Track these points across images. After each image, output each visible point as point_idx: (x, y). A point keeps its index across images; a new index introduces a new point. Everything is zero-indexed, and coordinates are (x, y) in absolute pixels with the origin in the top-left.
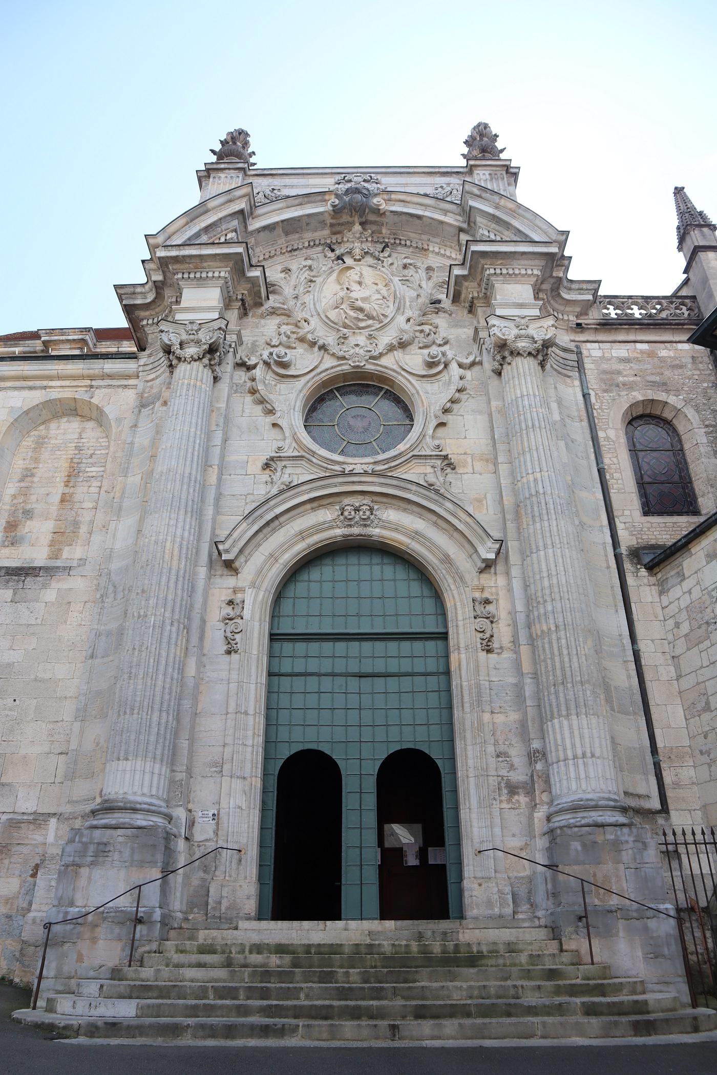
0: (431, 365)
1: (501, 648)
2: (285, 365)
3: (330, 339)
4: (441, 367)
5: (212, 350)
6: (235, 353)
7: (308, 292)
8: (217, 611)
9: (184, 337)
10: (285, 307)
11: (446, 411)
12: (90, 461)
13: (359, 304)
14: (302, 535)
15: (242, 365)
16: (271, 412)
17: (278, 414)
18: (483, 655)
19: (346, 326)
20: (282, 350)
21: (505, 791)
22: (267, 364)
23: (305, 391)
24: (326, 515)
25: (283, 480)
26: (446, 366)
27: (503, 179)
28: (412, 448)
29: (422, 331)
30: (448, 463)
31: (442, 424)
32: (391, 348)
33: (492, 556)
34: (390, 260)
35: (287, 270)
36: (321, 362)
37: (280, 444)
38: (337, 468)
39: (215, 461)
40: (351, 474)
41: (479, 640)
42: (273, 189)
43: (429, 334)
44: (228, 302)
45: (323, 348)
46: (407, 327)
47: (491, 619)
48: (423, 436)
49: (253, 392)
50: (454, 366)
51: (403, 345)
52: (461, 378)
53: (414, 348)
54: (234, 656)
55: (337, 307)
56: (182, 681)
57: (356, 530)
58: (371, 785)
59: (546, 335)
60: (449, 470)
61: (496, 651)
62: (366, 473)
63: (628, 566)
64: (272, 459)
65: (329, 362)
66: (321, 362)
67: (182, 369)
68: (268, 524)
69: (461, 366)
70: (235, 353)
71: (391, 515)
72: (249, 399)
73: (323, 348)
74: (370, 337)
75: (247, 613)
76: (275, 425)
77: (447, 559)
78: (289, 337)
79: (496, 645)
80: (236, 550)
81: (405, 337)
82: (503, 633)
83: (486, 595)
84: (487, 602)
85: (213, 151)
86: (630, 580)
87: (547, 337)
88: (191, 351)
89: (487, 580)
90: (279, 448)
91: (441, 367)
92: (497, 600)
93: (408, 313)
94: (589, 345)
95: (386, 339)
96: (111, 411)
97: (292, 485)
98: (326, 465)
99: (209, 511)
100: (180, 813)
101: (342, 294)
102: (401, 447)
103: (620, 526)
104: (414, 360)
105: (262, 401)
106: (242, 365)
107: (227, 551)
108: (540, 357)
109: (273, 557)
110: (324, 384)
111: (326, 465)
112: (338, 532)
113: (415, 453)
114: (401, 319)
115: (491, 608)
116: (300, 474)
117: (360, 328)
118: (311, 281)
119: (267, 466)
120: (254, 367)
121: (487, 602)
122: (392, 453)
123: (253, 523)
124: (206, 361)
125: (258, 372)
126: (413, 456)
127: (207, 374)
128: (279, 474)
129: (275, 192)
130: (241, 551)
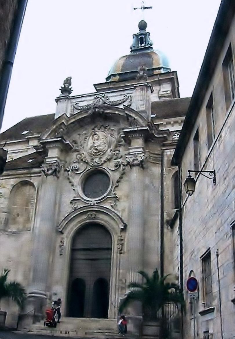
0: (116, 166)
1: (124, 252)
2: (77, 170)
3: (89, 160)
4: (118, 166)
5: (55, 170)
6: (64, 167)
7: (85, 142)
8: (58, 244)
9: (48, 167)
10: (78, 148)
11: (118, 182)
12: (32, 198)
13: (96, 148)
14: (79, 222)
15: (66, 170)
16: (73, 185)
17: (74, 186)
18: (119, 255)
19: (94, 155)
20: (77, 164)
21: (120, 289)
22: (72, 170)
23: (81, 179)
24: (84, 217)
25: (75, 207)
26: (120, 166)
27: (144, 90)
28: (108, 195)
29: (114, 154)
30: (116, 199)
31: (117, 186)
32: (105, 162)
33: (123, 228)
34: (109, 127)
35: (79, 134)
36: (86, 168)
37: (75, 195)
38: (88, 202)
39: (58, 203)
40: (91, 205)
41: (118, 250)
42: (76, 103)
43: (116, 155)
44: (62, 151)
45: (87, 163)
46: (110, 154)
47: (122, 245)
48: (111, 190)
49: (69, 179)
50: (122, 166)
51: (109, 160)
52: (124, 170)
53: (112, 160)
54: (62, 256)
55: (90, 149)
56: (49, 263)
57: (91, 221)
58: (92, 286)
59: (141, 159)
60: (117, 201)
61: (123, 253)
62: (94, 205)
63: (165, 226)
64: (72, 200)
65: (89, 168)
66: (86, 168)
67: (49, 177)
68: (70, 220)
69: (124, 165)
70: (64, 167)
71: (101, 216)
72: (68, 181)
73: (87, 163)
74: (100, 159)
75: (64, 245)
76: (74, 190)
77: (114, 229)
78: (78, 160)
79: (123, 252)
80: (62, 229)
81: (109, 157)
82: (125, 249)
83: (122, 238)
84: (122, 240)
85: (60, 89)
86: (165, 230)
87: (142, 160)
88: (50, 172)
89: (123, 234)
90: (74, 197)
91: (118, 166)
92: (125, 239)
93: (111, 148)
94: (166, 151)
95: (104, 158)
96: (36, 184)
97: (78, 208)
98: (85, 202)
99: (56, 217)
100: (48, 293)
101: (92, 144)
102: (105, 195)
103: (165, 214)
104: (111, 165)
105: (70, 182)
106: (66, 170)
107: (60, 229)
108: (141, 165)
109: (72, 228)
110: (87, 174)
111: (84, 201)
112: (88, 221)
113: (108, 197)
114: (109, 150)
115: (122, 242)
116: (80, 205)
117: (97, 155)
118: (86, 138)
119: (71, 203)
120: (69, 171)
121: (122, 240)
122: (103, 196)
123: (67, 220)
124: (54, 174)
125: (69, 172)
126: (107, 197)
127: (55, 177)
128: (74, 205)
129: (77, 104)
130: (63, 229)
